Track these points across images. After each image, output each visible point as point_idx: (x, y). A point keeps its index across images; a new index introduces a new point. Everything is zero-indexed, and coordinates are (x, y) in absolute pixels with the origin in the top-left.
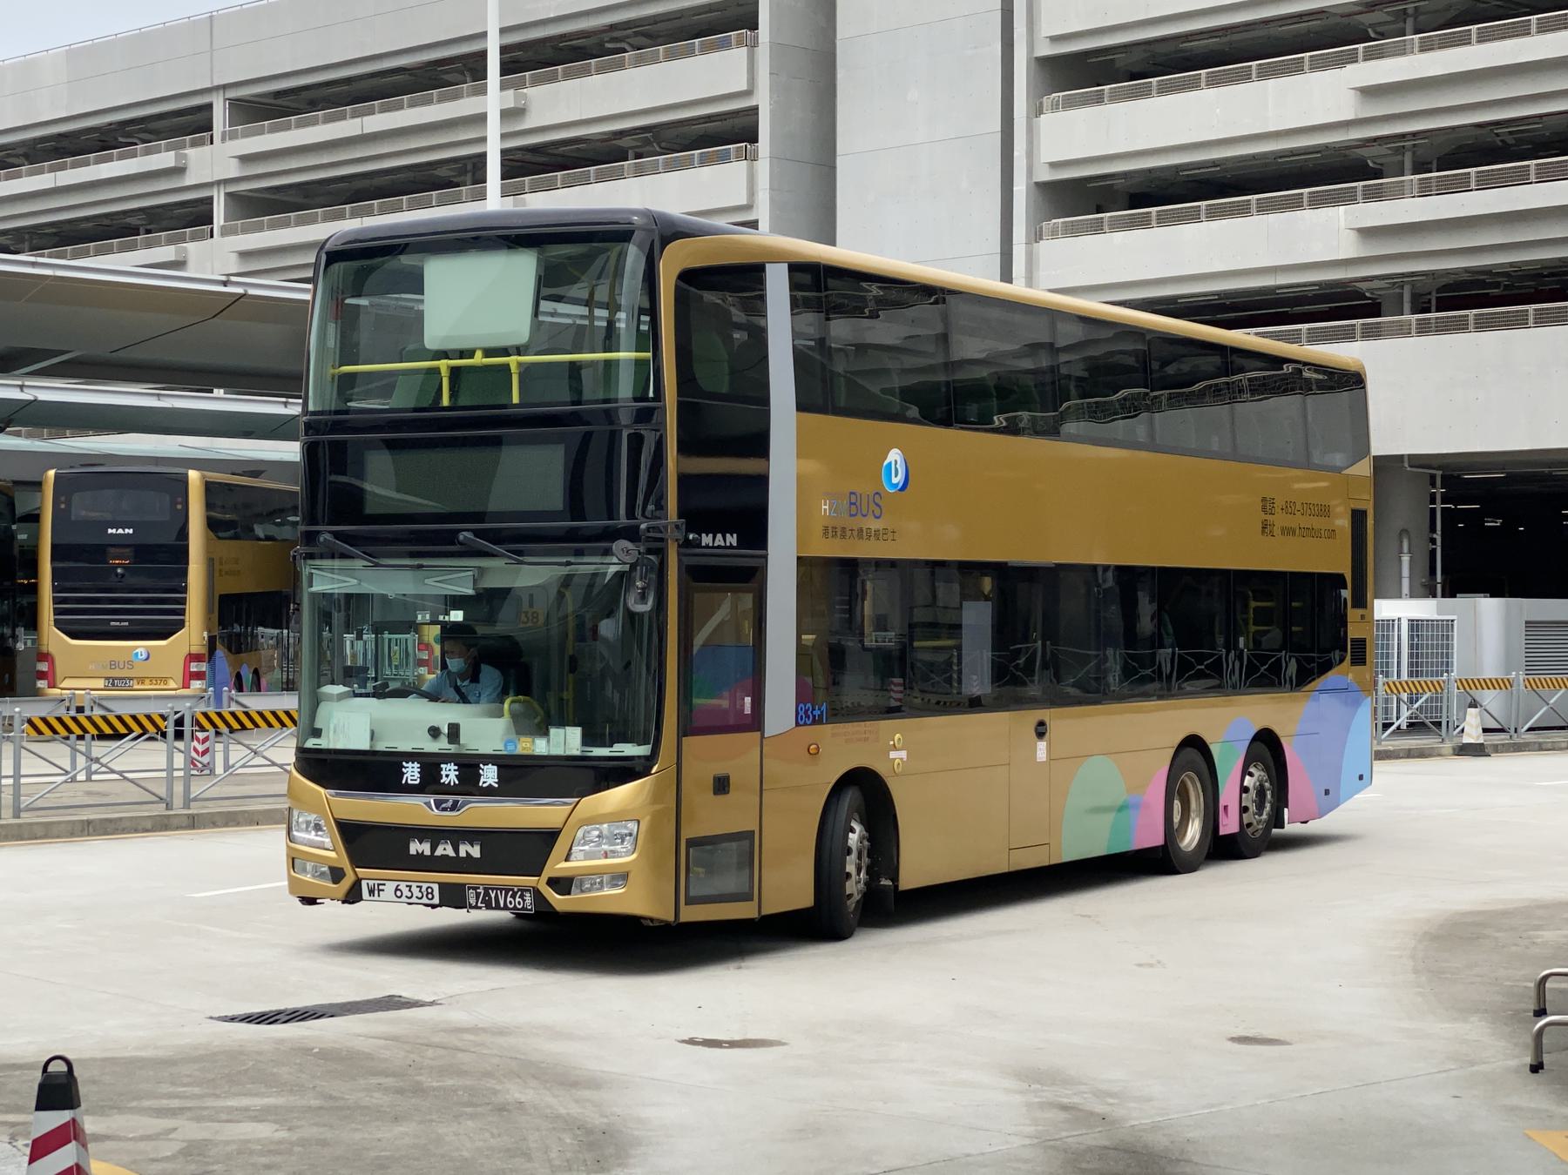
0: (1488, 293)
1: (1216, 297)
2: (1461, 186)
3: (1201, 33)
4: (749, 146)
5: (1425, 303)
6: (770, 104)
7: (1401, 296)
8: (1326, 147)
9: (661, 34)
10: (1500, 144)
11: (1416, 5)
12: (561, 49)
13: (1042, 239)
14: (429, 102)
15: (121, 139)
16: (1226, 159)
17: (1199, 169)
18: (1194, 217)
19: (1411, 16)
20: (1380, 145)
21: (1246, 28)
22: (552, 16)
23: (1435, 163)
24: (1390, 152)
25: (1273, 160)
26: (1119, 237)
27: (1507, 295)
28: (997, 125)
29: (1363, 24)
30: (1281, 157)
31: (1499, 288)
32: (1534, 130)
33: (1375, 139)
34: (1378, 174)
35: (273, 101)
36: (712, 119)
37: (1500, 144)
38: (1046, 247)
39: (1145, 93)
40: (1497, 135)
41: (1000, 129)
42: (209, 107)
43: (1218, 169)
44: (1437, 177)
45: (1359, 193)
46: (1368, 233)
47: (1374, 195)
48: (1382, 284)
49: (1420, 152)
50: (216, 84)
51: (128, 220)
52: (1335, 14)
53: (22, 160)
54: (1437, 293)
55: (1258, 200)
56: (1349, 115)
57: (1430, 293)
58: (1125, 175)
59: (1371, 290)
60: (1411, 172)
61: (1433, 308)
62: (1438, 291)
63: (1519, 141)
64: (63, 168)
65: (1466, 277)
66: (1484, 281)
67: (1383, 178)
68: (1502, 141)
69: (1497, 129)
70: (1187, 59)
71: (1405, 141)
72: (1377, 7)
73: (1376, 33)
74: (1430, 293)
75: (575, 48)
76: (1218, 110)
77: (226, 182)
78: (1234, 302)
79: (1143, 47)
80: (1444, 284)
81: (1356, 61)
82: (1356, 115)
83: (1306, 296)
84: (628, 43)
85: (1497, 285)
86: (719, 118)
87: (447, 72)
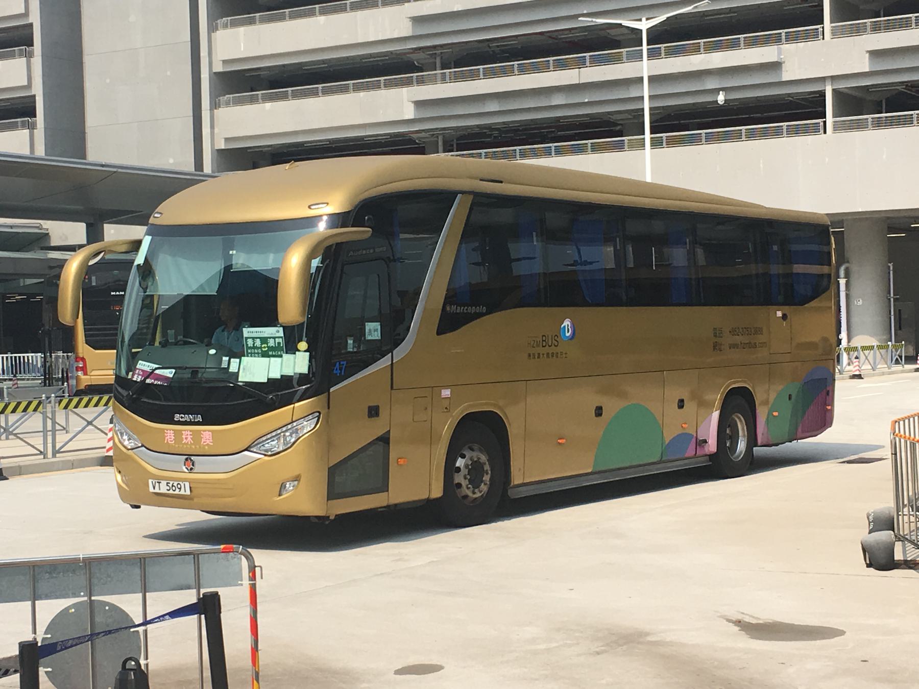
1: (328, 143)
2: (474, 76)
4: (27, 49)
7: (437, 142)
8: (391, 52)
10: (491, 53)
13: (220, 107)
16: (330, 60)
18: (315, 94)
20: (423, 52)
23: (453, 63)
24: (429, 57)
25: (359, 60)
26: (268, 105)
28: (187, 36)
30: (364, 59)
33: (420, 49)
37: (491, 53)
39: (282, 18)
44: (455, 72)
45: (415, 80)
47: (421, 81)
48: (427, 135)
59: (419, 138)
60: (440, 68)
63: (503, 52)
68: (492, 51)
74: (453, 140)
83: (381, 142)
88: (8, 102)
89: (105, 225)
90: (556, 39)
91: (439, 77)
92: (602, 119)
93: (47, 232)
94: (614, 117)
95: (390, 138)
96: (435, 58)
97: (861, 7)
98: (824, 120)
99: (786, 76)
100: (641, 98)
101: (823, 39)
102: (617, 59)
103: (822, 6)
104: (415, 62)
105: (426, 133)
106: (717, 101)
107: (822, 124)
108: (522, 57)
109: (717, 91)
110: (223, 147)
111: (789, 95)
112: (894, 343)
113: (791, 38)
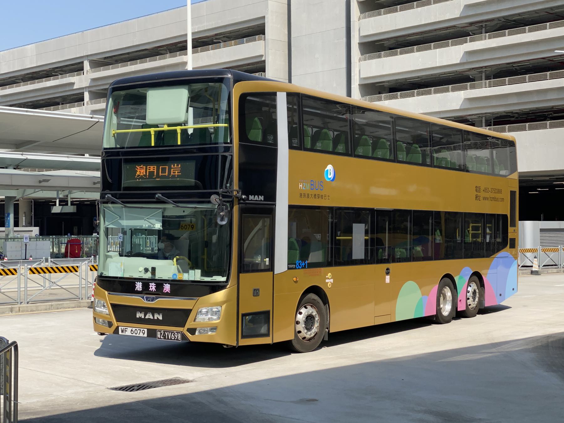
3: (414, 34)
5: (489, 123)
7: (482, 120)
9: (232, 37)
10: (514, 69)
11: (485, 24)
12: (199, 42)
14: (156, 60)
15: (53, 74)
19: (483, 27)
21: (429, 32)
22: (196, 31)
23: (492, 76)
29: (468, 30)
31: (514, 118)
32: (526, 65)
33: (473, 69)
34: (473, 80)
35: (103, 60)
36: (250, 64)
37: (514, 69)
40: (514, 67)
42: (82, 63)
43: (420, 79)
44: (493, 81)
47: (472, 87)
48: (476, 117)
49: (487, 72)
50: (84, 55)
51: (56, 100)
52: (459, 27)
53: (21, 81)
54: (493, 120)
58: (388, 81)
60: (484, 79)
61: (492, 125)
64: (34, 83)
65: (504, 114)
66: (509, 115)
67: (475, 81)
68: (515, 69)
70: (408, 43)
71: (483, 69)
72: (473, 25)
73: (472, 33)
74: (491, 120)
75: (203, 42)
76: (420, 59)
77: (88, 87)
79: (394, 39)
80: (495, 117)
81: (467, 43)
82: (467, 60)
84: (222, 40)
85: (513, 117)
86: (252, 64)
87: (161, 50)
95: (454, 119)
96: (482, 73)
104: (470, 76)
105: (475, 115)
108: (533, 71)
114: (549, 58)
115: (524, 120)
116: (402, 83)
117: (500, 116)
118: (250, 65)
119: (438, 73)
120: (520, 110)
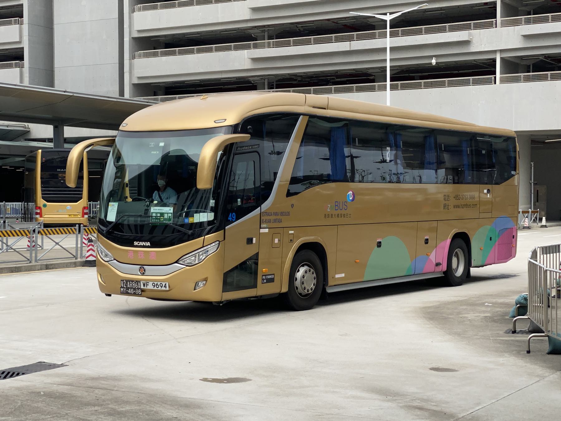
0: (292, 83)
2: (288, 44)
4: (19, 19)
6: (28, 4)
8: (238, 29)
17: (192, 35)
18: (192, 52)
23: (275, 36)
26: (164, 58)
27: (299, 84)
28: (116, 15)
30: (222, 32)
32: (310, 26)
33: (255, 27)
34: (256, 39)
36: (5, 8)
37: (298, 30)
38: (136, 61)
40: (297, 27)
41: (118, 17)
43: (199, 35)
46: (255, 60)
47: (255, 47)
48: (258, 78)
49: (270, 32)
55: (215, 47)
56: (248, 17)
57: (273, 82)
60: (267, 39)
61: (275, 88)
62: (276, 81)
63: (305, 30)
65: (288, 77)
66: (293, 78)
68: (299, 29)
69: (298, 25)
74: (273, 82)
76: (200, 14)
78: (205, 84)
82: (250, 17)
83: (231, 82)
85: (296, 80)
86: (6, 8)
88: (7, 51)
89: (64, 127)
90: (336, 23)
91: (266, 45)
92: (361, 71)
93: (29, 130)
94: (370, 71)
96: (265, 33)
97: (519, 9)
98: (495, 76)
99: (473, 49)
100: (386, 60)
101: (496, 27)
102: (373, 37)
103: (496, 7)
106: (432, 63)
107: (493, 78)
109: (431, 57)
110: (136, 82)
111: (474, 60)
112: (533, 210)
113: (477, 27)
114: (332, 20)
115: (306, 83)
116: (180, 39)
117: (283, 78)
118: (3, 9)
119: (220, 30)
120: (305, 73)
